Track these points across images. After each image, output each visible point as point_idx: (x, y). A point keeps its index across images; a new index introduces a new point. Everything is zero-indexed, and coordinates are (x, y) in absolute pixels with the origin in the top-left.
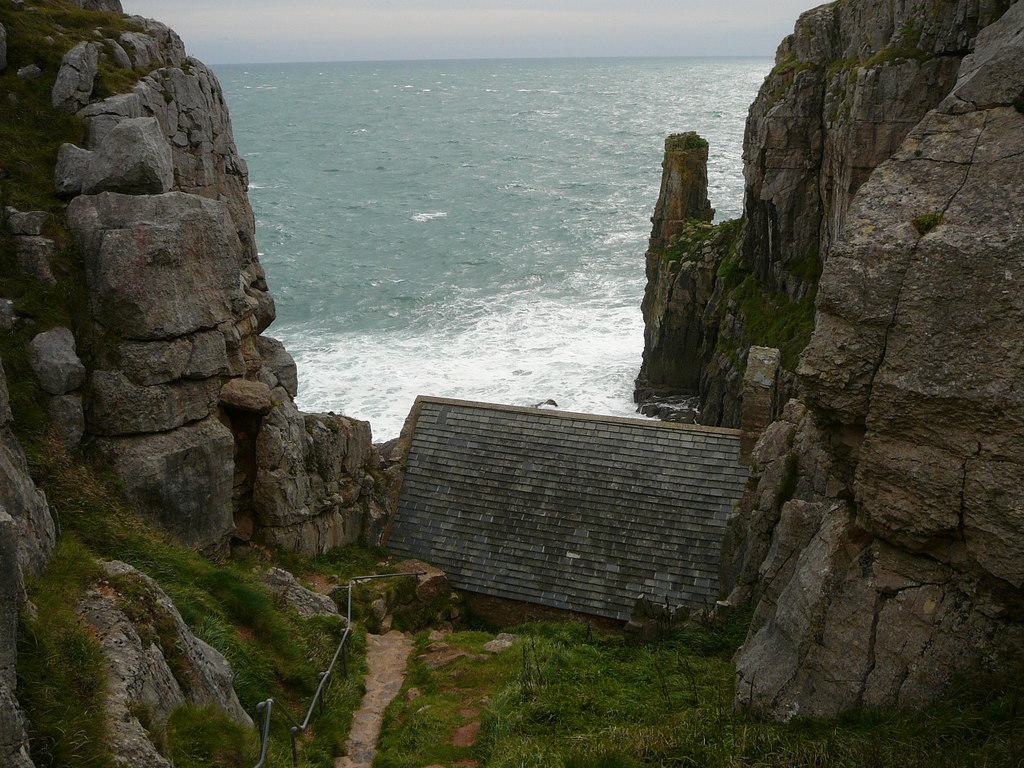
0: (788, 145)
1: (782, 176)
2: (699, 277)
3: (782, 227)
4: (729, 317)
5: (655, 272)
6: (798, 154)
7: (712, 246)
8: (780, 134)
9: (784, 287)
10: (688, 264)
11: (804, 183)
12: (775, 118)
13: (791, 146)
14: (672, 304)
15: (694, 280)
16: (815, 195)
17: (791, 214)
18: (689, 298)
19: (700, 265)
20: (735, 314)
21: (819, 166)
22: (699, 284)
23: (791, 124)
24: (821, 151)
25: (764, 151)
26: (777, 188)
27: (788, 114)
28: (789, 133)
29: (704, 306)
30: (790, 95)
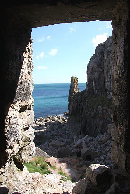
0: (97, 67)
1: (96, 73)
2: (78, 100)
3: (96, 83)
4: (86, 103)
5: (70, 100)
6: (99, 68)
7: (80, 95)
8: (95, 65)
9: (98, 94)
10: (76, 98)
11: (100, 74)
12: (94, 62)
13: (98, 67)
14: (74, 106)
15: (77, 101)
16: (103, 76)
17: (98, 80)
18: (77, 104)
19: (78, 98)
20: (88, 102)
21: (103, 70)
22: (78, 101)
23: (97, 63)
24: (104, 67)
25: (92, 68)
26: (95, 75)
27: (96, 61)
28: (97, 64)
29: (80, 106)
30: (97, 58)
